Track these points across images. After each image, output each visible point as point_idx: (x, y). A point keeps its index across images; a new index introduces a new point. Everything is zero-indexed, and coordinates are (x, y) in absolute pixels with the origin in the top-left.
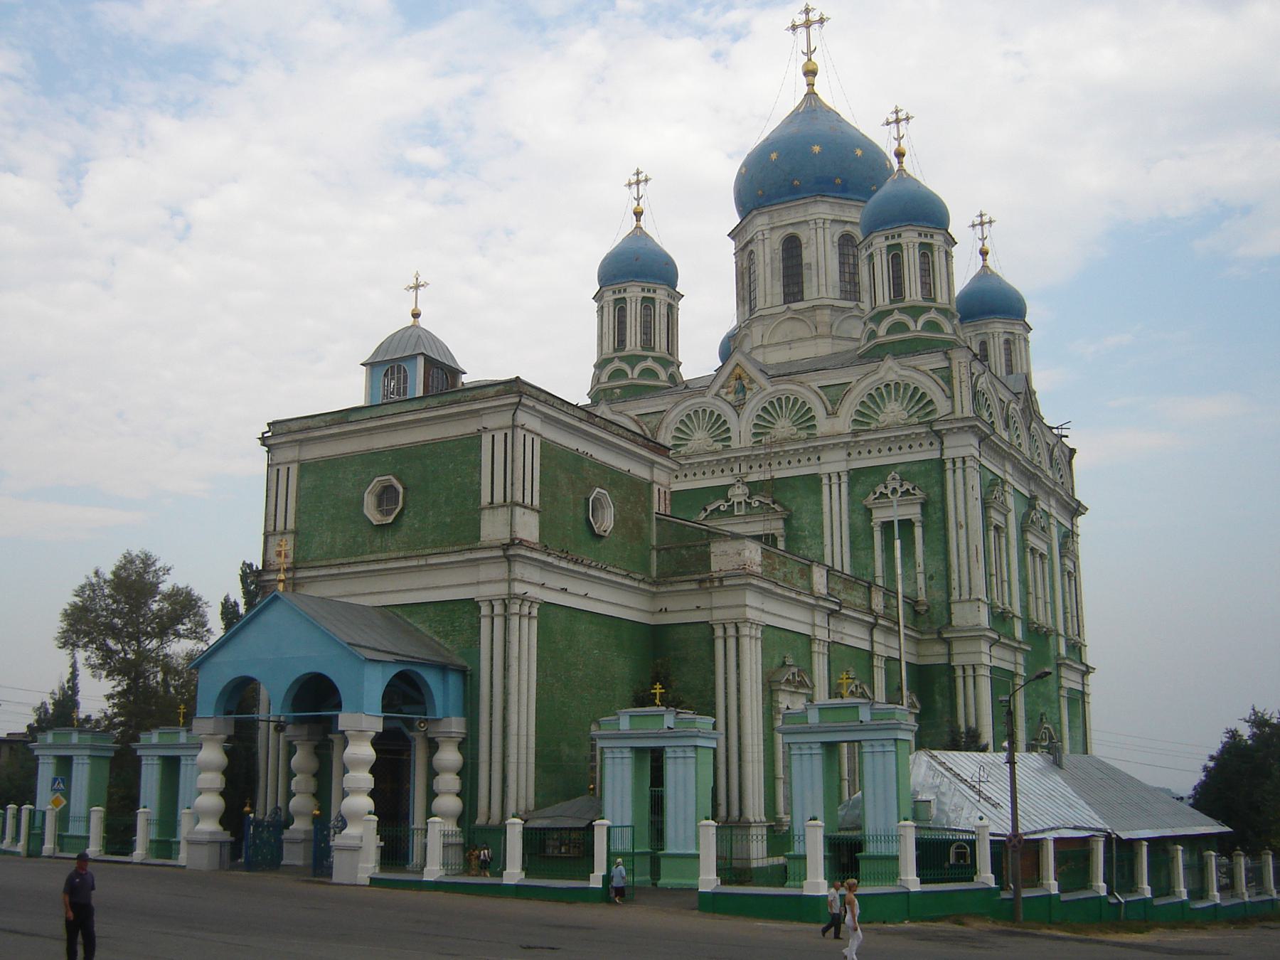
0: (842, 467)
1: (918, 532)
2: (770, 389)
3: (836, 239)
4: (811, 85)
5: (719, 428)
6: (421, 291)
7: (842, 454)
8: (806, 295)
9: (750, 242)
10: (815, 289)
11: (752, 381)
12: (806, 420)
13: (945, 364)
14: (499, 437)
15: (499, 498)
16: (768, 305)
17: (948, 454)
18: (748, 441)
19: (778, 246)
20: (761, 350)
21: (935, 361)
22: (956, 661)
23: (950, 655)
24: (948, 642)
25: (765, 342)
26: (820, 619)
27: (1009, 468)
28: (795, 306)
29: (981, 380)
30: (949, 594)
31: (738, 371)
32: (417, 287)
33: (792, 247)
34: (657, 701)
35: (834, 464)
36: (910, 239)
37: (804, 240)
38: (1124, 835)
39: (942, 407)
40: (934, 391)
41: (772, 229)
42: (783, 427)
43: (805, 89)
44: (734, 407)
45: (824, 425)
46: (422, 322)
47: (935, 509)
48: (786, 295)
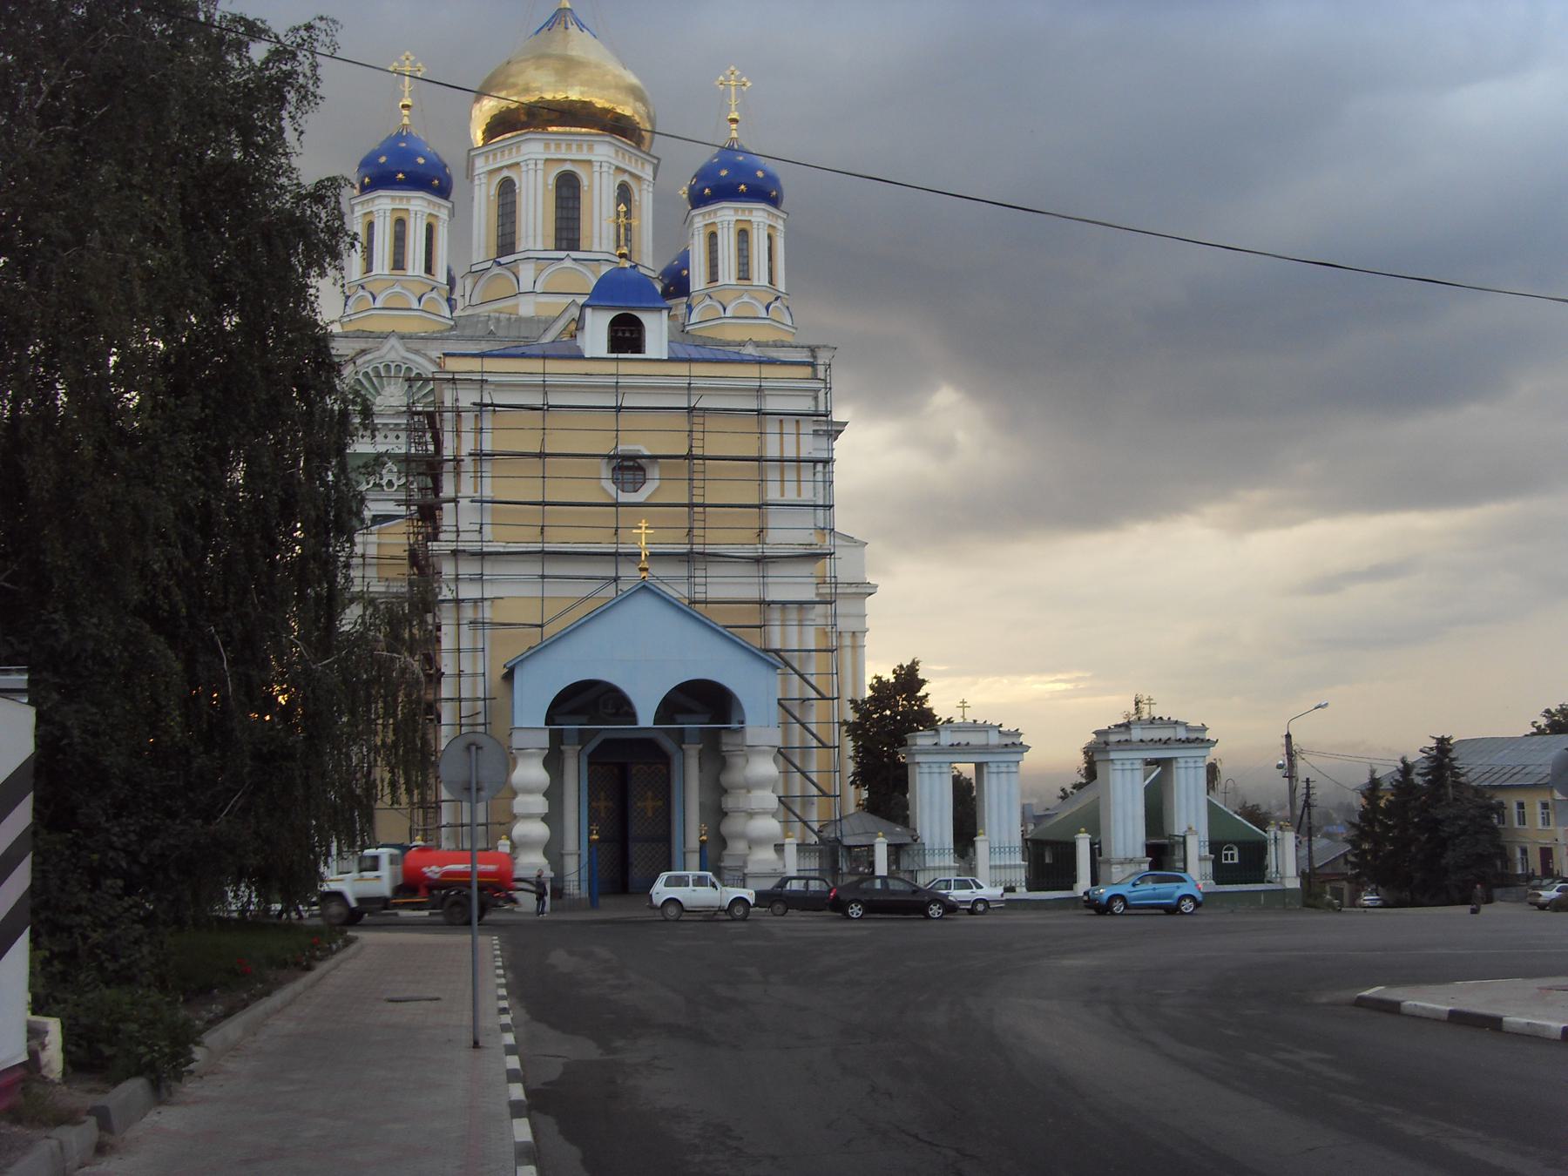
8: (583, 244)
19: (551, 181)
20: (531, 298)
25: (538, 289)
28: (574, 254)
37: (585, 181)
48: (558, 239)
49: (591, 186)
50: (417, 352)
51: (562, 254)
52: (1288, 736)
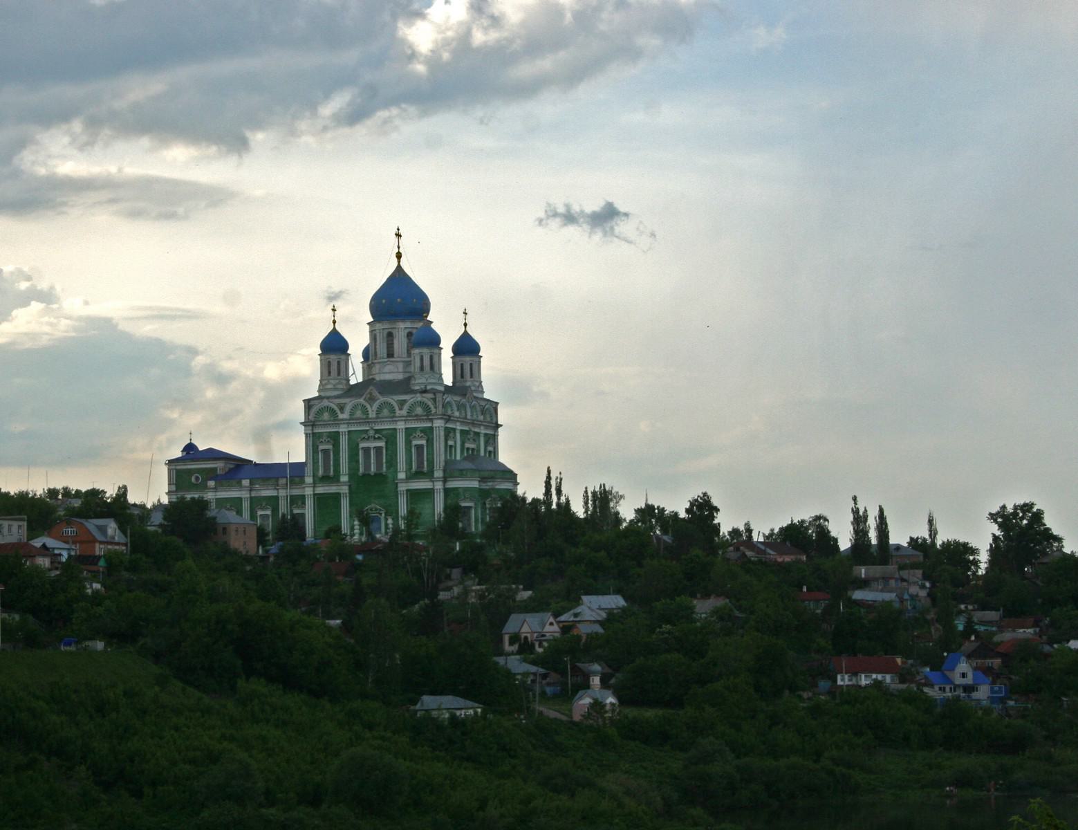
0: (403, 427)
1: (425, 449)
4: (399, 262)
5: (365, 412)
7: (403, 423)
12: (392, 411)
13: (434, 397)
17: (434, 425)
18: (374, 416)
19: (385, 335)
21: (431, 396)
22: (436, 488)
23: (434, 485)
24: (433, 482)
30: (433, 468)
35: (401, 426)
36: (426, 352)
39: (433, 411)
40: (430, 404)
42: (385, 412)
43: (396, 264)
45: (398, 412)
47: (430, 442)
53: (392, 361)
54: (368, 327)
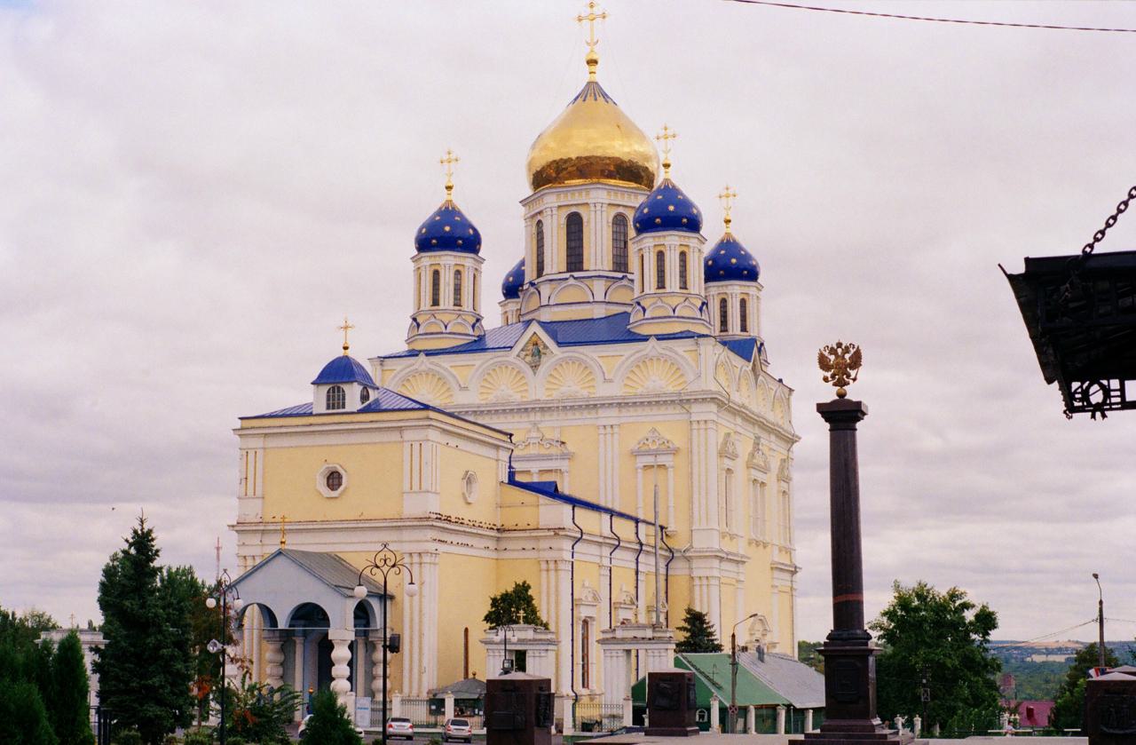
2: (561, 356)
3: (611, 220)
6: (349, 330)
7: (614, 412)
9: (540, 213)
10: (593, 261)
11: (546, 347)
14: (416, 446)
15: (416, 488)
16: (555, 271)
19: (563, 221)
20: (547, 309)
23: (691, 568)
25: (552, 303)
26: (606, 551)
27: (739, 420)
28: (576, 274)
29: (722, 357)
30: (691, 523)
31: (534, 339)
32: (346, 328)
33: (575, 225)
34: (521, 621)
37: (585, 220)
38: (798, 706)
41: (559, 207)
44: (532, 367)
46: (349, 353)
48: (569, 264)
49: (588, 222)
50: (437, 365)
51: (567, 275)
52: (733, 636)
53: (575, 278)
54: (522, 210)
